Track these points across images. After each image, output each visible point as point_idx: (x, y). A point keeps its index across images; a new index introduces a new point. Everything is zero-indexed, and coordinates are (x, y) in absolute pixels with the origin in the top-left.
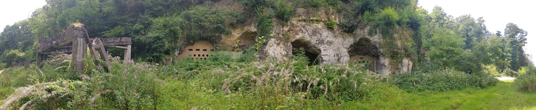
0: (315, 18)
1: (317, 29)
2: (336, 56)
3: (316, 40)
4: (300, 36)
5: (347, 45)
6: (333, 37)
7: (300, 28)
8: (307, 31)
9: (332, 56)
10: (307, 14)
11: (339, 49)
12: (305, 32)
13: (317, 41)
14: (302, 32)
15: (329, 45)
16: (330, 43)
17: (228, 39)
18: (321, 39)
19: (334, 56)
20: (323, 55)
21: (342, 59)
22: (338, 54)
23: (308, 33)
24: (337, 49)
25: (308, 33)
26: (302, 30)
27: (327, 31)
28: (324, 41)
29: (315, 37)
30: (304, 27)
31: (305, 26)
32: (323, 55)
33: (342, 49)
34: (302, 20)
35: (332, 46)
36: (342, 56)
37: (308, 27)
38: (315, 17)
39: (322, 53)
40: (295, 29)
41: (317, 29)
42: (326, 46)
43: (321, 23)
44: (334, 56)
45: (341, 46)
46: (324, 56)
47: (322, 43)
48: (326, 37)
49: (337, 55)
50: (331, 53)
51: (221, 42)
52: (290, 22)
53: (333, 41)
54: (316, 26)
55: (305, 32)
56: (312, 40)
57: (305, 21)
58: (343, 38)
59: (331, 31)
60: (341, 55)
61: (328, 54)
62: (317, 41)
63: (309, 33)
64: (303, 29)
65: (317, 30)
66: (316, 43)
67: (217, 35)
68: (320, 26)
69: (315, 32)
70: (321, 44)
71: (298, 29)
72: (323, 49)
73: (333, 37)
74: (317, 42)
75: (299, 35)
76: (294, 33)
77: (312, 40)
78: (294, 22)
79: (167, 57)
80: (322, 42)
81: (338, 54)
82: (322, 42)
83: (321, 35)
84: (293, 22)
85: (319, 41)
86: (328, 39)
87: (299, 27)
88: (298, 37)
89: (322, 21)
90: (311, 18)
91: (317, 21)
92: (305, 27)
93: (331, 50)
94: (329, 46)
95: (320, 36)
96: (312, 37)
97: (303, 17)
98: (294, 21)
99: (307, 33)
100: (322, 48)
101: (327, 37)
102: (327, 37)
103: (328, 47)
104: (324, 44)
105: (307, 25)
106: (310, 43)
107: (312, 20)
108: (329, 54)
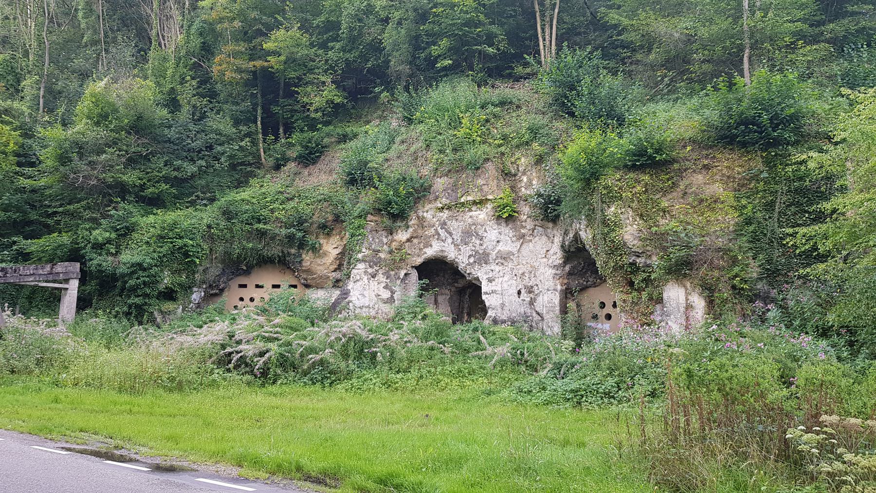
0: (470, 198)
1: (474, 224)
2: (523, 291)
3: (468, 255)
4: (436, 249)
5: (555, 257)
6: (514, 239)
7: (436, 230)
8: (451, 234)
9: (511, 292)
10: (453, 190)
11: (533, 270)
12: (444, 238)
13: (470, 257)
14: (438, 239)
15: (502, 264)
16: (505, 258)
17: (318, 261)
18: (481, 252)
19: (519, 293)
20: (486, 293)
21: (540, 299)
22: (532, 287)
23: (453, 239)
24: (531, 272)
25: (453, 239)
26: (439, 234)
27: (496, 227)
28: (488, 255)
29: (468, 248)
30: (443, 225)
31: (445, 223)
32: (486, 293)
33: (542, 269)
34: (443, 208)
35: (510, 265)
36: (541, 291)
37: (453, 225)
38: (469, 195)
39: (484, 289)
40: (427, 233)
41: (474, 224)
42: (493, 268)
43: (488, 206)
44: (519, 293)
45: (545, 260)
46: (487, 296)
47: (483, 262)
48: (495, 243)
49: (530, 290)
50: (505, 286)
51: (304, 268)
52: (418, 217)
53: (515, 250)
54: (471, 217)
55: (444, 238)
56: (459, 257)
57: (449, 208)
58: (549, 238)
59: (507, 225)
60: (538, 289)
61: (498, 288)
62: (470, 257)
63: (455, 238)
64: (440, 231)
65: (473, 228)
66: (469, 264)
67: (293, 251)
68: (482, 215)
69: (468, 234)
70: (480, 264)
71: (432, 230)
72: (485, 277)
73: (514, 239)
74: (472, 260)
75: (431, 246)
76: (422, 244)
77: (459, 257)
78: (428, 216)
79: (168, 306)
80: (483, 258)
81: (532, 287)
82: (483, 258)
83: (481, 240)
84: (425, 214)
85: (475, 257)
86: (501, 247)
87: (434, 226)
88: (430, 252)
89: (487, 200)
90: (462, 200)
91: (475, 203)
92: (446, 225)
93: (506, 278)
94: (501, 268)
95: (478, 242)
96: (460, 250)
97: (444, 201)
98: (427, 212)
99: (450, 240)
100: (481, 273)
101: (498, 242)
102: (498, 242)
103: (497, 268)
104: (490, 263)
105: (450, 218)
106: (457, 263)
107: (463, 204)
108: (500, 289)
